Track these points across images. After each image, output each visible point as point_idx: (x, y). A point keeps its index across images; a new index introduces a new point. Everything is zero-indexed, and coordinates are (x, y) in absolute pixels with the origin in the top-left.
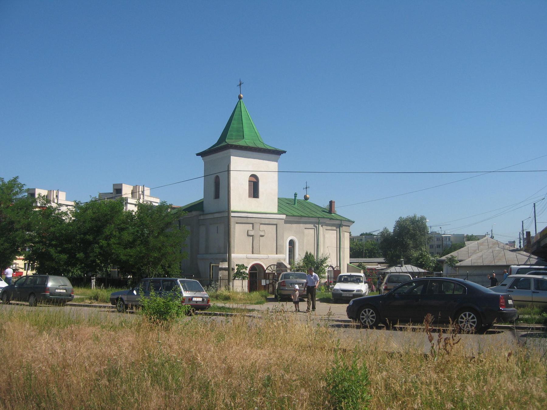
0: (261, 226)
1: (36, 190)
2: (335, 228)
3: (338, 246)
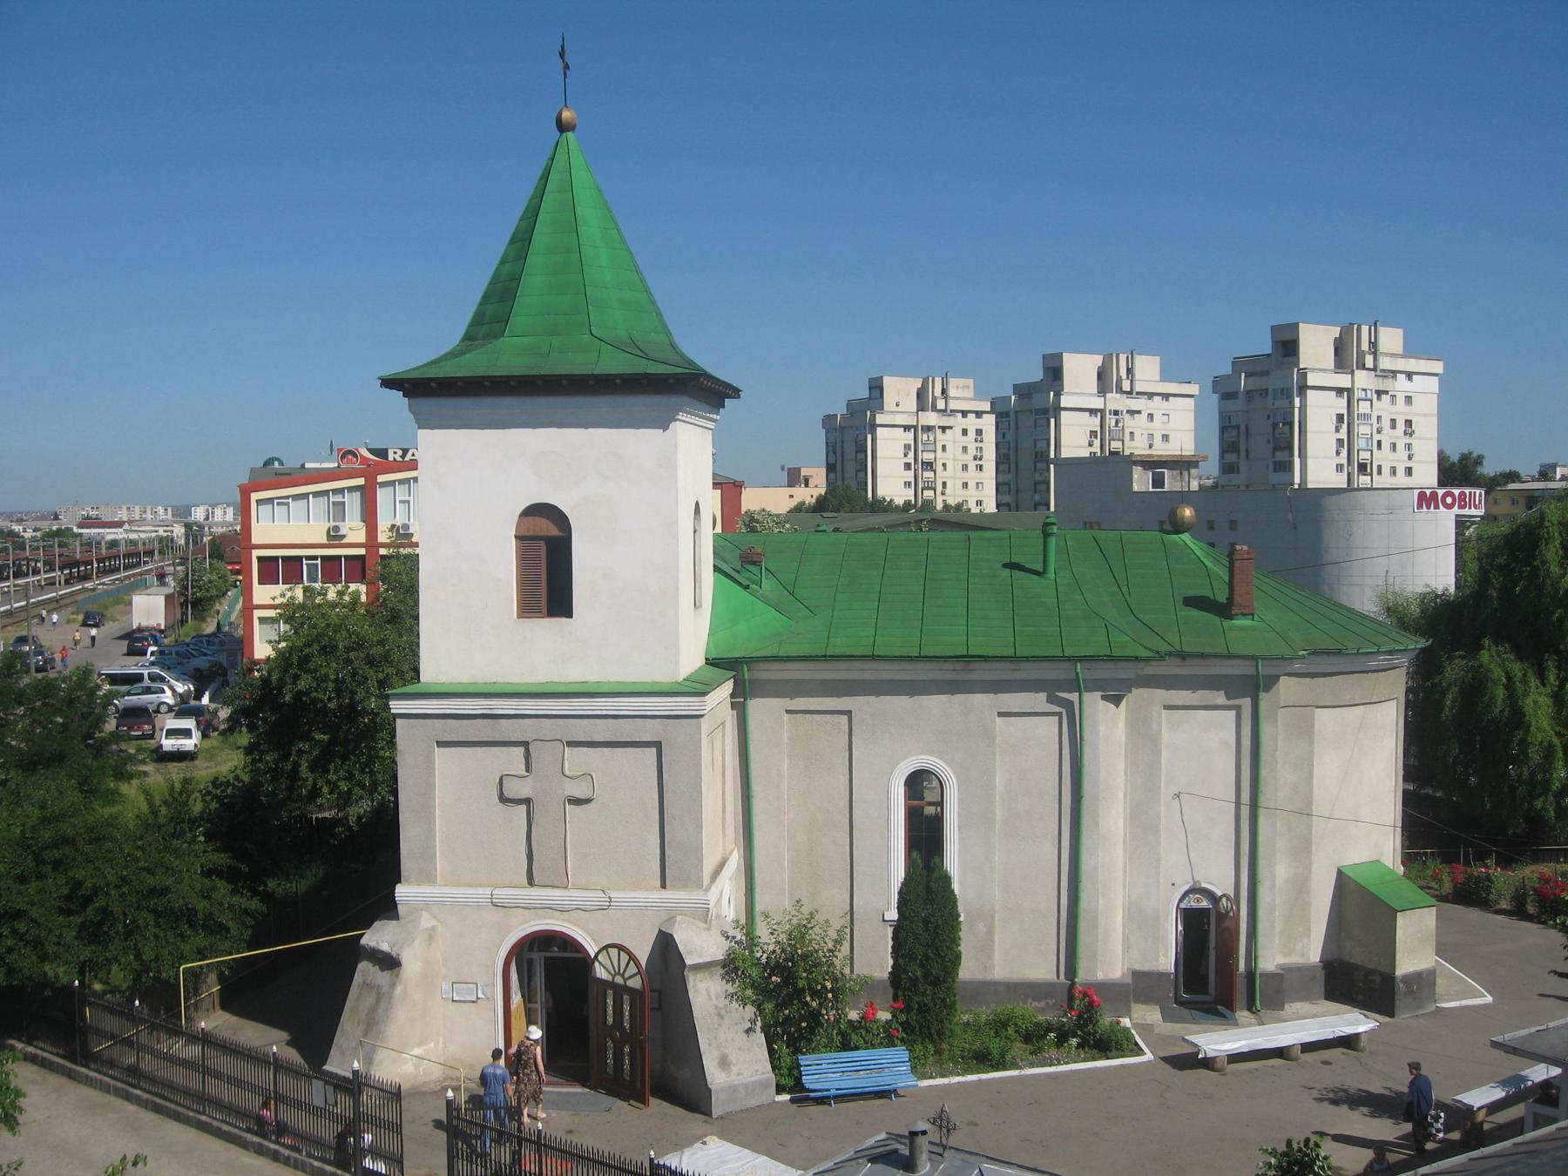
1: (1065, 355)
2: (1220, 697)
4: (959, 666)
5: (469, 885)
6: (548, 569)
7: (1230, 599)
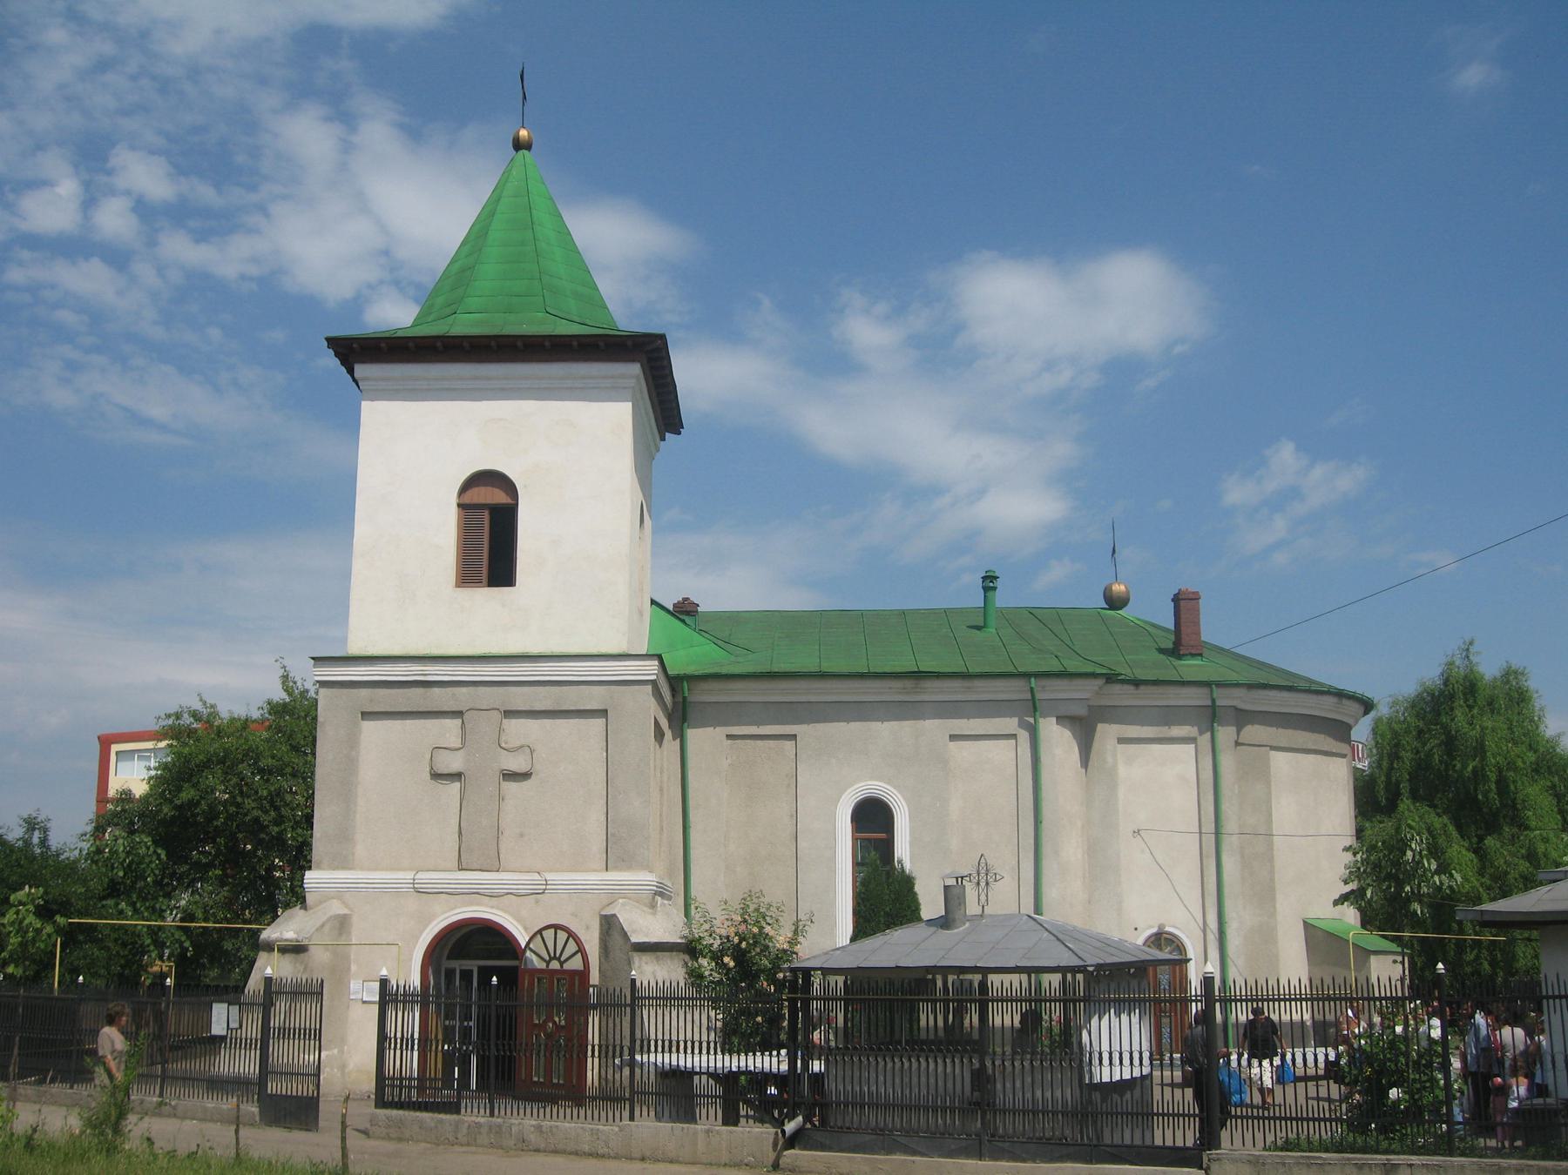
0: (513, 725)
3: (1209, 827)
4: (909, 684)
5: (392, 869)
6: (491, 538)
7: (1178, 643)
